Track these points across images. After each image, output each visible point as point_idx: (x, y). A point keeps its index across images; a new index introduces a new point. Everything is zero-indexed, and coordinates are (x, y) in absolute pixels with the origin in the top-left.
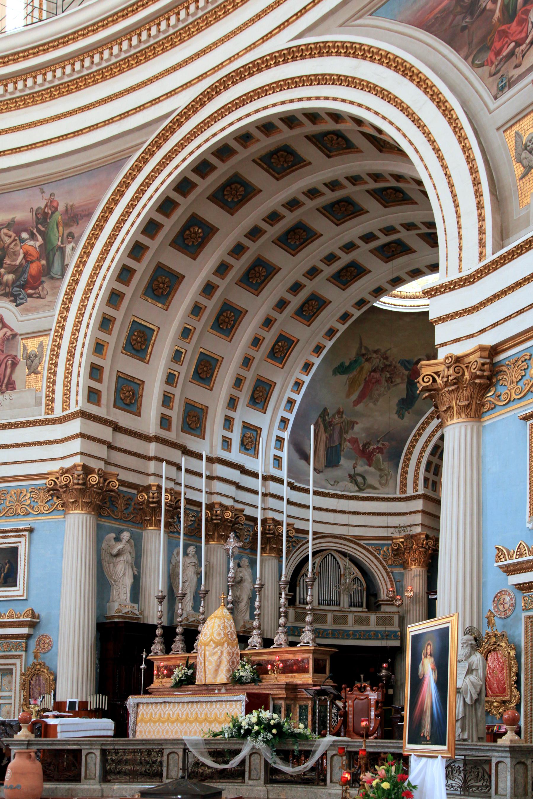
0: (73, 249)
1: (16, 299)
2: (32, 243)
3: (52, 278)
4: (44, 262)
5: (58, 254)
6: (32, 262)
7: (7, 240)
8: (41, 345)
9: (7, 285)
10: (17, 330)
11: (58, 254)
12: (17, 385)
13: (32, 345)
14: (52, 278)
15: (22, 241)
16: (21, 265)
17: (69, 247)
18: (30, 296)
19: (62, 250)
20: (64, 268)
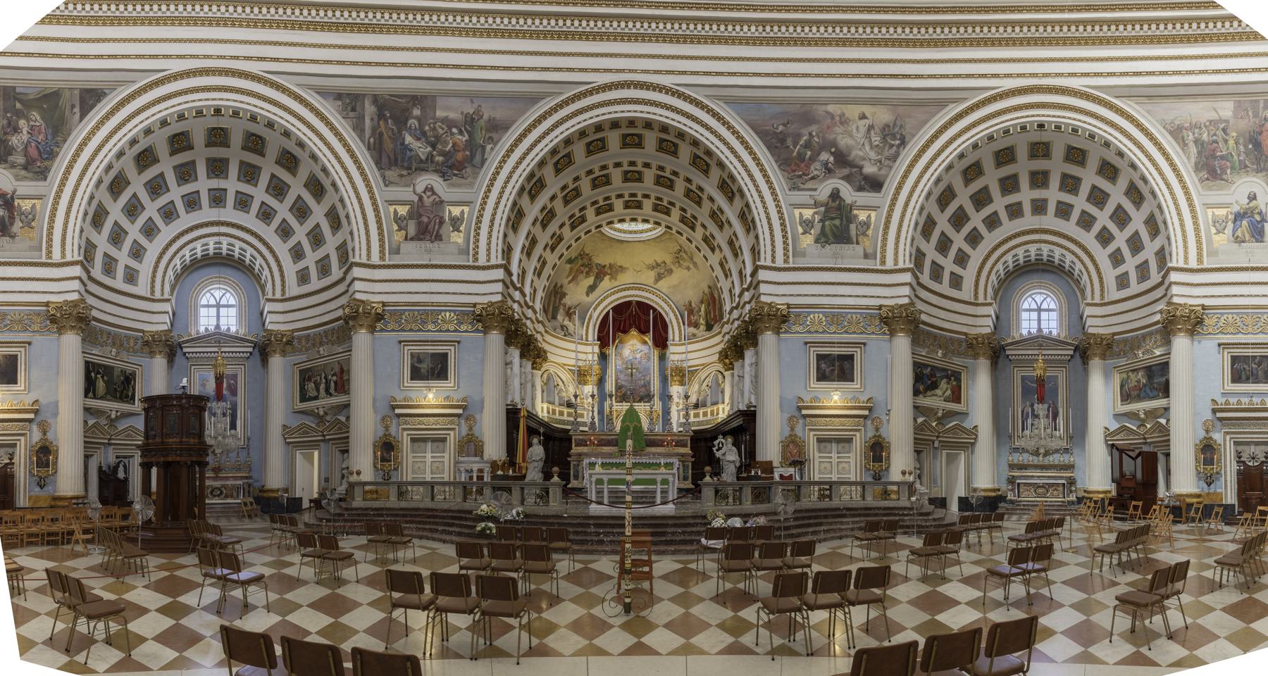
0: (492, 149)
1: (443, 175)
2: (460, 137)
3: (474, 166)
4: (468, 153)
5: (480, 149)
6: (459, 151)
7: (441, 131)
8: (463, 212)
9: (437, 163)
10: (443, 198)
11: (480, 149)
12: (444, 237)
13: (456, 211)
14: (474, 166)
15: (452, 134)
16: (449, 151)
17: (489, 147)
18: (455, 175)
19: (484, 148)
20: (483, 161)
